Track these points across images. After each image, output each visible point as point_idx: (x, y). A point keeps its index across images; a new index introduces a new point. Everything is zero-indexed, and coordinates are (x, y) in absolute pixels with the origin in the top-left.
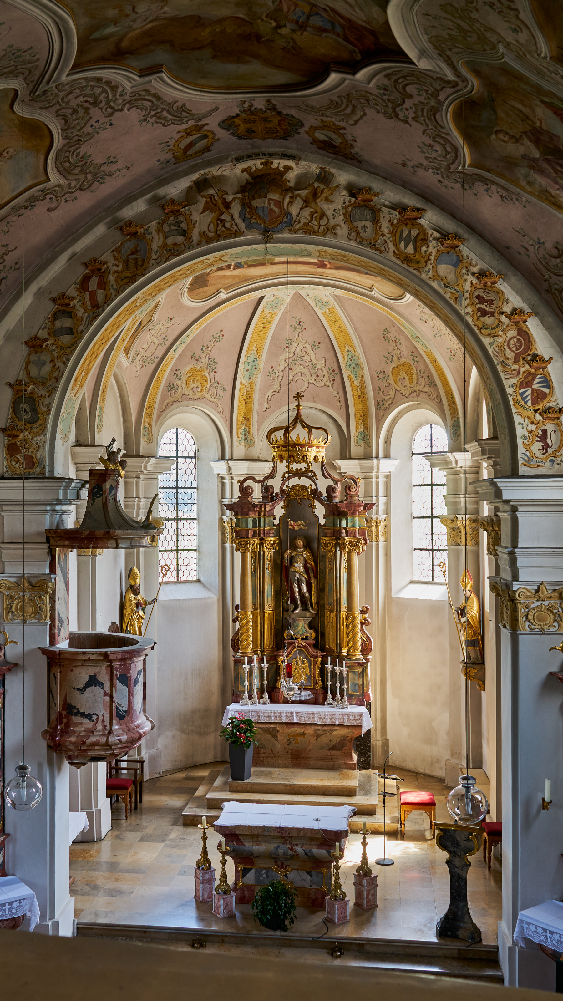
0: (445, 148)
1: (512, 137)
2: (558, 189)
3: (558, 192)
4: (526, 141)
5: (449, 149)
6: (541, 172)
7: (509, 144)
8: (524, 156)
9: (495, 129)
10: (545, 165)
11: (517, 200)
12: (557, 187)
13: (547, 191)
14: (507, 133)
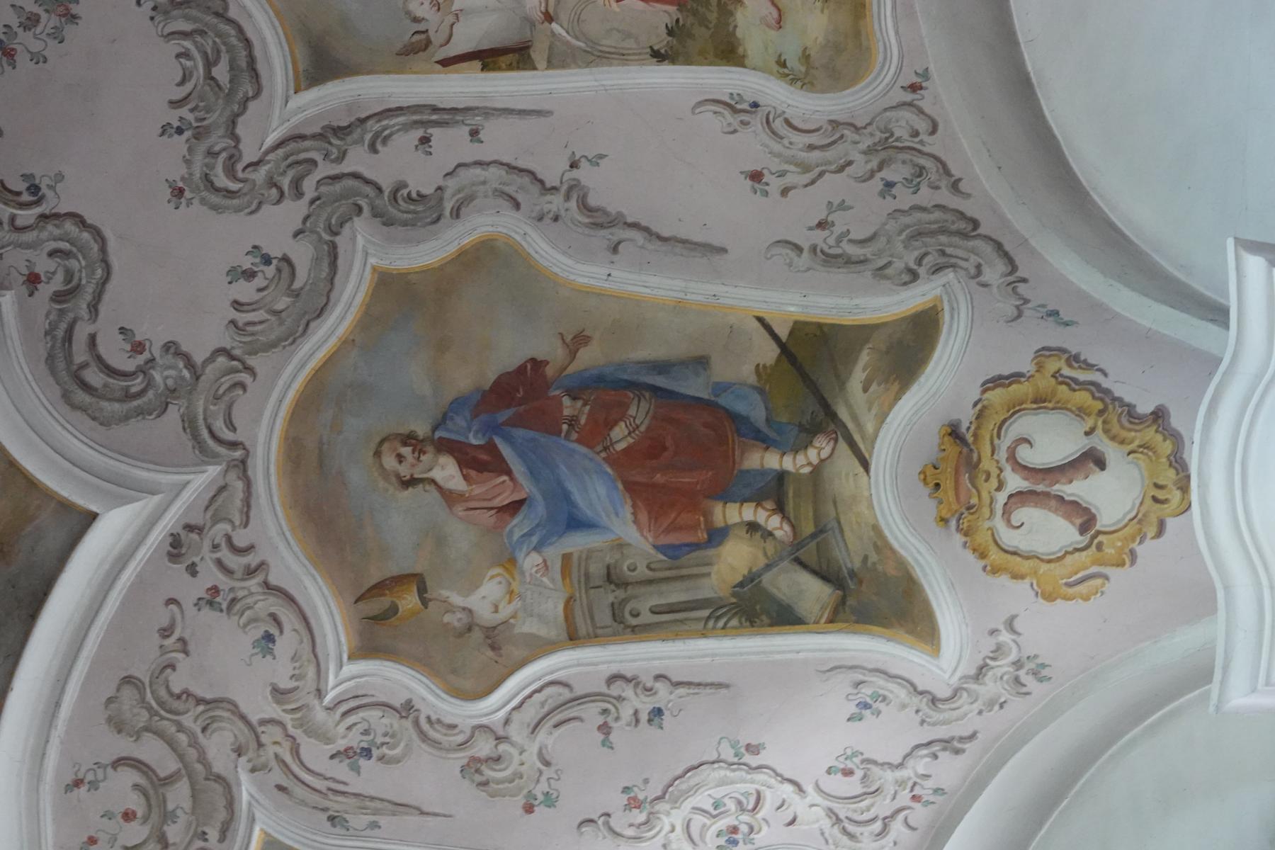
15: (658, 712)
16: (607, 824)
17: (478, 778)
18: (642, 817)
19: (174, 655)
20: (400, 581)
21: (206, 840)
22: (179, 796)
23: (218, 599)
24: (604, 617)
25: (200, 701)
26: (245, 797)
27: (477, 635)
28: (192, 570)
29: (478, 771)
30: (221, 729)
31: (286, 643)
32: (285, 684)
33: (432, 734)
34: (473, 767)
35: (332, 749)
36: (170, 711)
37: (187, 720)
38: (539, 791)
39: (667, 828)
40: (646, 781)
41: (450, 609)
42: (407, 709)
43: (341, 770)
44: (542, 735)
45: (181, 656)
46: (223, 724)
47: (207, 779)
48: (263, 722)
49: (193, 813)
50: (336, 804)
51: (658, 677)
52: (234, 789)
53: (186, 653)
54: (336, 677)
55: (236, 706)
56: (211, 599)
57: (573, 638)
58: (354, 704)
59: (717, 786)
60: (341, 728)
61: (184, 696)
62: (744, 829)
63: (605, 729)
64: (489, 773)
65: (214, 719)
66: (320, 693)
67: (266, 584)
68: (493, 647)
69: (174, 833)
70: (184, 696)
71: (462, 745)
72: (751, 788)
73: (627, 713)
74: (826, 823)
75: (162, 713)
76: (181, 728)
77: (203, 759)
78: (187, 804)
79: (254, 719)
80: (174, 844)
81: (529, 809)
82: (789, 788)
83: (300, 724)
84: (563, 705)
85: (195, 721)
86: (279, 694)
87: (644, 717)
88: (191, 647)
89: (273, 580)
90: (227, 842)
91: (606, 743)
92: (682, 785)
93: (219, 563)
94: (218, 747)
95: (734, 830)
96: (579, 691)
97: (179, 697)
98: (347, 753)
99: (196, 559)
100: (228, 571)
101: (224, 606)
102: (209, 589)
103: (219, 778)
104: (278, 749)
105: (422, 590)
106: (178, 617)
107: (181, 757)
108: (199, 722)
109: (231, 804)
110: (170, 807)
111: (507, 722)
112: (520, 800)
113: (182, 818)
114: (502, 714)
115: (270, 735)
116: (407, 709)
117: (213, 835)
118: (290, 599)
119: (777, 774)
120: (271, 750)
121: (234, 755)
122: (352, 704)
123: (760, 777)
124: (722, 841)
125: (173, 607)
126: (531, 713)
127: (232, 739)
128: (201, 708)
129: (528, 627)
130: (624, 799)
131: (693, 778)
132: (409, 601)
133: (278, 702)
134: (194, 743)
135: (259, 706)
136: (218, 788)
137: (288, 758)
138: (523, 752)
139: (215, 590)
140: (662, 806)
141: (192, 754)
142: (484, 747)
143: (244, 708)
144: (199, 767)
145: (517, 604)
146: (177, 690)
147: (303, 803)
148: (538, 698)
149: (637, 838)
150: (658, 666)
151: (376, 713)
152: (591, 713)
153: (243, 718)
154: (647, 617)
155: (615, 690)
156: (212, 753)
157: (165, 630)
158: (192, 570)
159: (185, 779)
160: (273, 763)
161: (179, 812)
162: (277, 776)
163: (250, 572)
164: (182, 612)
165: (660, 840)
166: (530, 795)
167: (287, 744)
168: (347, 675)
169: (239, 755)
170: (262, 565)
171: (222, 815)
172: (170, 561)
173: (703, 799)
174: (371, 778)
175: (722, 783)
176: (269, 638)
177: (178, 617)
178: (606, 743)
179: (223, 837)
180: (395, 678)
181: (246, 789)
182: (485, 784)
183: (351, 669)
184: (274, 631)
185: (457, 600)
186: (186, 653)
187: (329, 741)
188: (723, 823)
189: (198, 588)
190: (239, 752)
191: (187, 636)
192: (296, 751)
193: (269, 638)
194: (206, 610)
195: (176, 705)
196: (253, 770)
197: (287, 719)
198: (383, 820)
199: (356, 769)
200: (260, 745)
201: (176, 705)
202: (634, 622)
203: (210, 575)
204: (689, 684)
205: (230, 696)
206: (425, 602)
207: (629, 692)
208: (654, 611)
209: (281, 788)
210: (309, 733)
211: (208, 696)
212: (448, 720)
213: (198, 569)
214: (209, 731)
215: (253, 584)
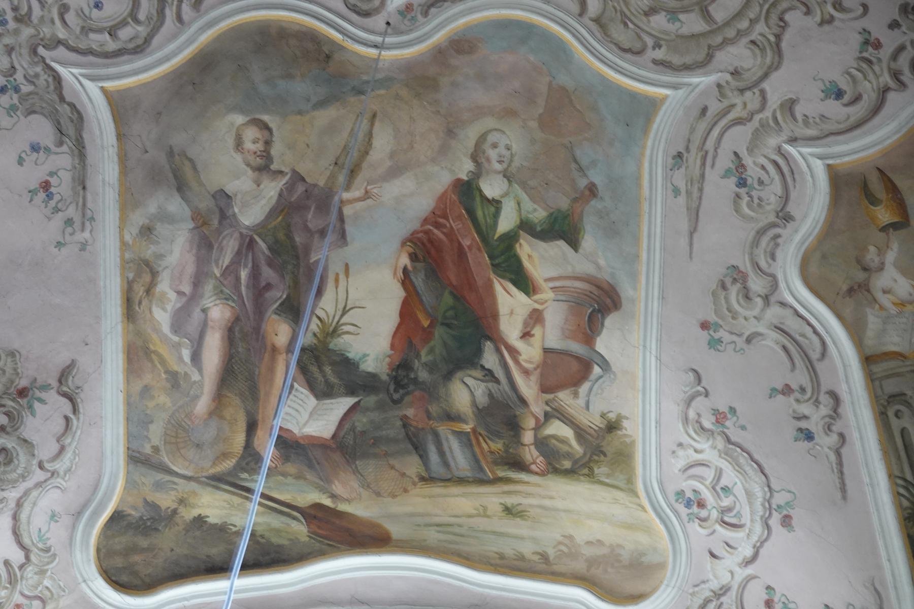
0: (123, 23)
1: (266, 156)
2: (180, 293)
3: (172, 296)
4: (272, 190)
5: (125, 33)
6: (205, 244)
7: (238, 158)
8: (223, 198)
9: (266, 118)
10: (230, 246)
11: (69, 222)
12: (187, 289)
13: (154, 274)
14: (268, 143)
15: (809, 436)
16: (698, 394)
17: (728, 281)
18: (707, 424)
19: (819, 12)
20: (901, 205)
21: (654, 48)
22: (692, 23)
23: (870, 49)
24: (891, 387)
25: (778, 37)
26: (695, 80)
27: (861, 276)
28: (894, 25)
29: (735, 280)
30: (755, 55)
31: (835, 109)
32: (799, 110)
33: (765, 240)
34: (738, 276)
35: (743, 153)
36: (768, 12)
37: (761, 27)
38: (721, 334)
39: (698, 446)
40: (743, 428)
41: (881, 252)
42: (784, 217)
43: (725, 161)
44: (775, 335)
45: (818, 18)
46: (759, 59)
47: (709, 47)
48: (763, 93)
49: (677, 36)
50: (694, 159)
51: (842, 436)
52: (701, 71)
53: (822, 23)
54: (812, 155)
55: (777, 68)
56: (870, 42)
57: (868, 360)
58: (787, 172)
59: (746, 490)
60: (762, 161)
61: (782, 24)
62: (703, 513)
63: (787, 390)
64: (734, 290)
65: (763, 50)
66: (793, 140)
67: (886, 90)
68: (851, 291)
69: (659, 21)
70: (782, 24)
71: (757, 266)
72: (746, 519)
73: (805, 409)
74: (715, 585)
75: (766, 6)
76: (753, 22)
77: (726, 42)
78: (685, 31)
79: (766, 85)
80: (649, 21)
81: (705, 326)
82: (749, 552)
83: (763, 125)
84: (804, 352)
85: (761, 34)
86: (789, 106)
87: (803, 424)
88: (826, 28)
89: (891, 96)
90: (652, 65)
91: (774, 392)
92: (743, 459)
93: (901, 48)
94: (739, 55)
95: (701, 505)
96: (819, 367)
97: (781, 19)
98: (740, 166)
99: (904, 29)
100: (895, 56)
101: (865, 55)
102: (878, 40)
103: (710, 57)
104: (739, 108)
105: (894, 226)
106: (852, 15)
107: (727, 24)
108: (759, 37)
109: (687, 68)
110: (682, 17)
111: (783, 304)
112: (712, 318)
113: (672, 27)
114: (790, 300)
115: (752, 99)
116: (784, 217)
117: (659, 54)
118: (876, 110)
119: (762, 543)
120: (738, 101)
121: (731, 69)
122: (785, 169)
123: (758, 528)
124: (689, 494)
125: (861, 8)
126: (793, 325)
127: (746, 66)
128: (772, 39)
129: (873, 321)
130: (723, 408)
131: (751, 469)
132: (884, 215)
133: (782, 106)
134: (740, 34)
135: (777, 89)
136: (701, 57)
137: (732, 116)
138: (754, 319)
139: (878, 45)
140: (720, 443)
141: (731, 33)
142: (757, 285)
143: (775, 76)
144: (719, 39)
145: (893, 310)
146: (787, 17)
147: (692, 130)
148: (808, 331)
149: (686, 420)
150: (854, 436)
151: (779, 190)
152: (801, 378)
153: (766, 76)
154: (895, 424)
155: (824, 398)
156: (731, 49)
157: (840, 4)
158: (894, 25)
159: (708, 28)
160: (726, 103)
161: (678, 24)
162: (715, 107)
163: (896, 75)
164: (856, 19)
165: (686, 440)
166: (718, 327)
167: (744, 114)
168: (813, 166)
169: (732, 74)
170: (903, 85)
171: (676, 60)
172: (901, 5)
173: (730, 477)
174: (719, 188)
175: (749, 495)
176: (839, 94)
177: (852, 15)
178: (774, 392)
179: (655, 62)
180: (814, 205)
181: (702, 81)
182: (724, 287)
183: (819, 167)
184: (846, 98)
185: (891, 256)
186: (822, 23)
187: (750, 150)
188: (707, 495)
189: (879, 32)
190: (735, 73)
191: (836, 23)
192: (739, 122)
193: (839, 94)
194: (859, 39)
195: (774, 18)
196: (719, 86)
197: (768, 113)
198: (682, 200)
199: (727, 174)
200: (742, 91)
201: (774, 18)
202: (891, 413)
203: (890, 41)
204: (840, 464)
205: (785, 63)
206: (884, 229)
207: (824, 410)
208: (903, 431)
209: (704, 110)
210: (756, 135)
211: (784, 45)
212: (779, 254)
213: (896, 30)
214: (752, 47)
215: (886, 78)
